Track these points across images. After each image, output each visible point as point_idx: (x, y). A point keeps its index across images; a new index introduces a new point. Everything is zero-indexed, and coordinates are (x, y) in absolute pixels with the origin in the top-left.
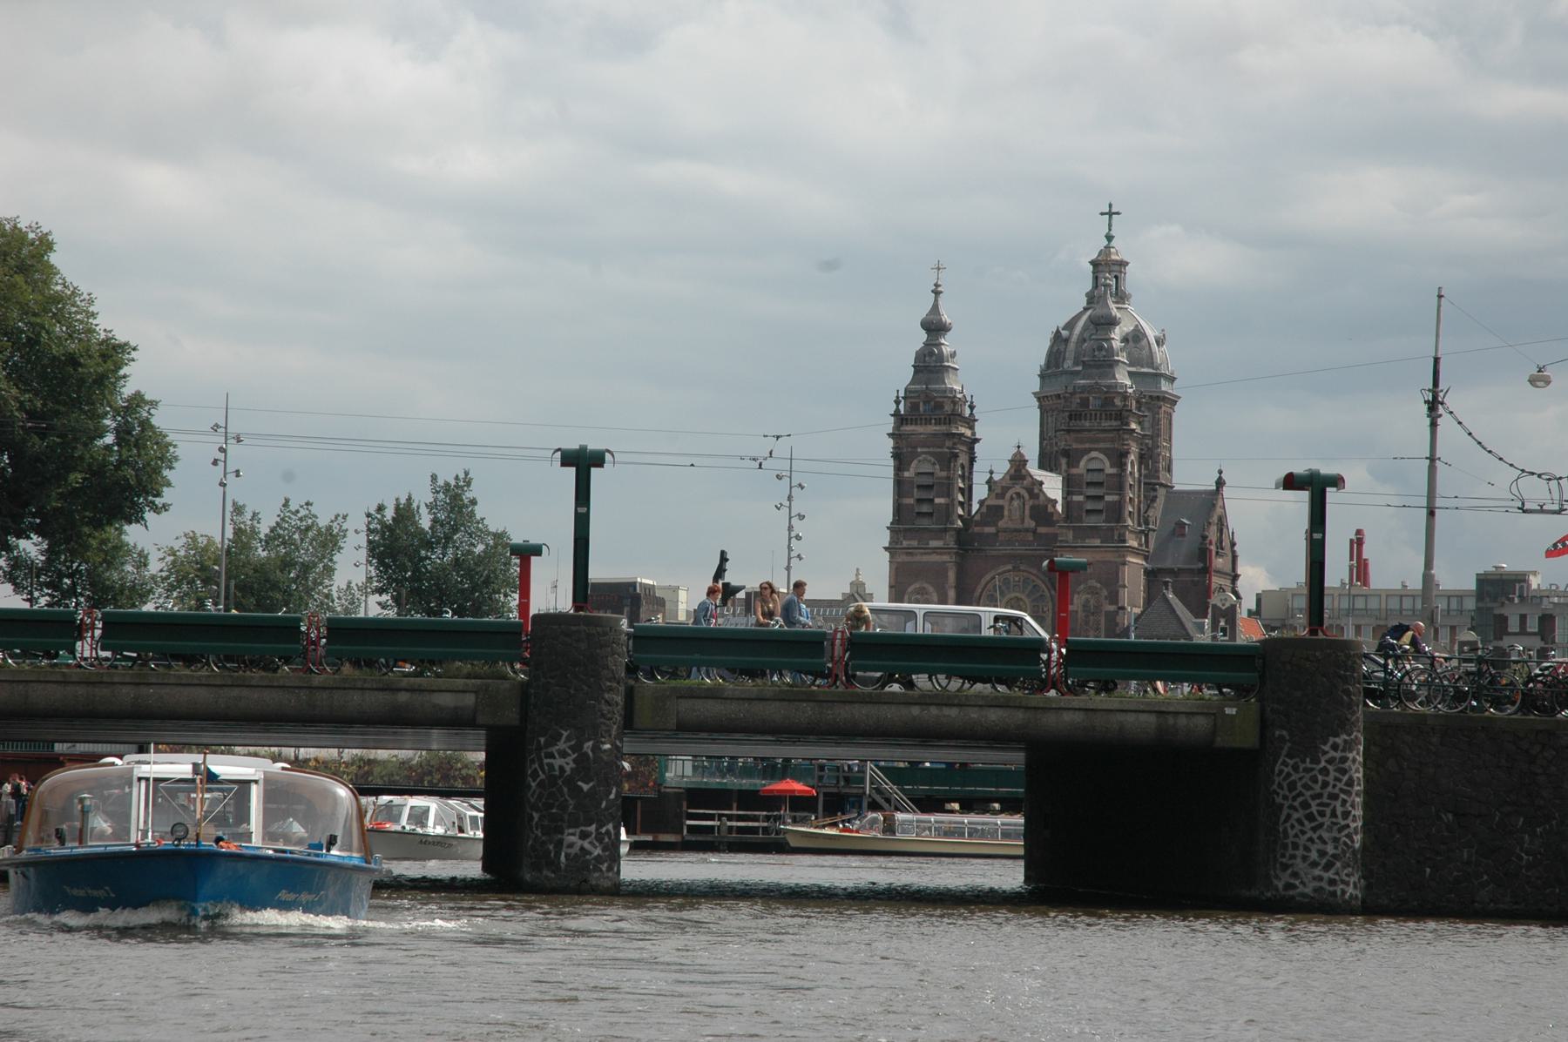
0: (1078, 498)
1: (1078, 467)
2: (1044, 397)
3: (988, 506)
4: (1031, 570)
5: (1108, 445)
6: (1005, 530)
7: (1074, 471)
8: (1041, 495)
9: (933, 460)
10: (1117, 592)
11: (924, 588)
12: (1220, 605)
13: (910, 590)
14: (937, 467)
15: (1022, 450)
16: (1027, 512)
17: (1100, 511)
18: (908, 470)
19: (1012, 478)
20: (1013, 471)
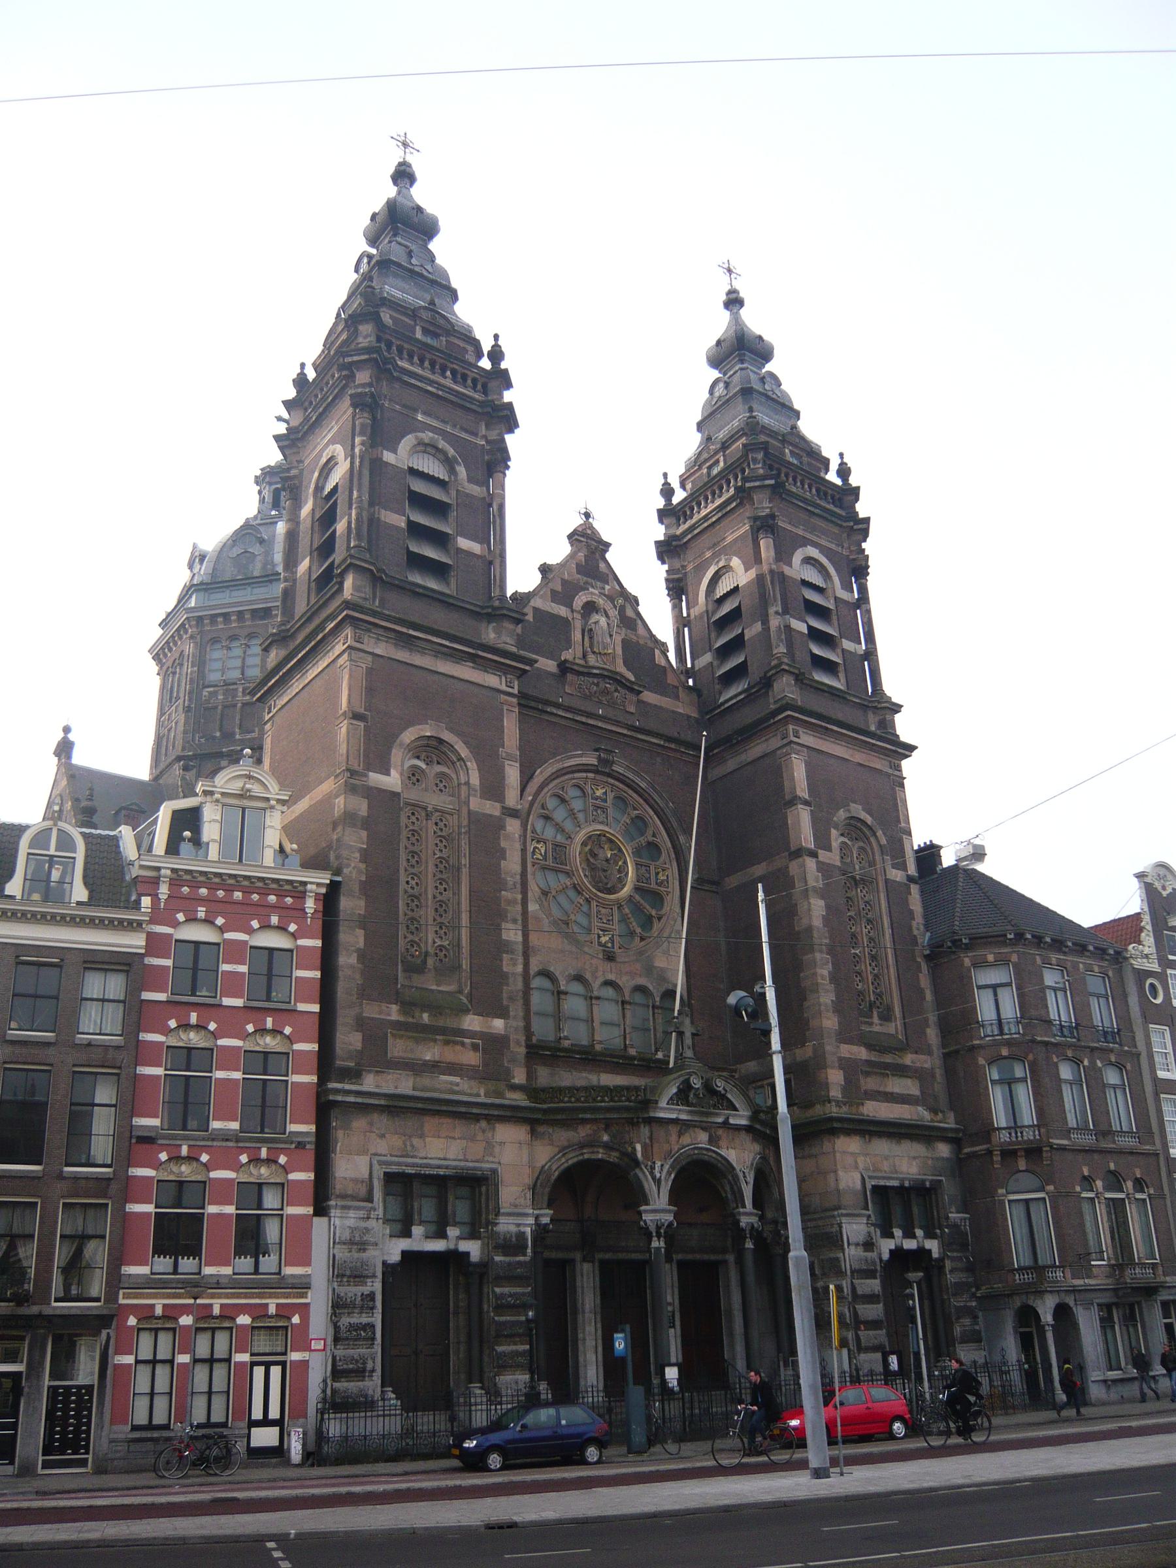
0: (800, 627)
1: (790, 565)
2: (213, 618)
3: (534, 608)
4: (637, 780)
5: (833, 546)
6: (585, 673)
7: (787, 570)
8: (639, 622)
9: (451, 452)
10: (901, 841)
11: (441, 741)
12: (1158, 885)
13: (409, 736)
14: (462, 471)
15: (596, 525)
16: (619, 651)
17: (829, 667)
18: (395, 451)
19: (580, 569)
20: (581, 556)
